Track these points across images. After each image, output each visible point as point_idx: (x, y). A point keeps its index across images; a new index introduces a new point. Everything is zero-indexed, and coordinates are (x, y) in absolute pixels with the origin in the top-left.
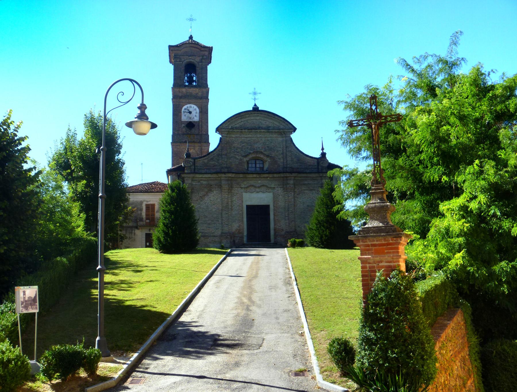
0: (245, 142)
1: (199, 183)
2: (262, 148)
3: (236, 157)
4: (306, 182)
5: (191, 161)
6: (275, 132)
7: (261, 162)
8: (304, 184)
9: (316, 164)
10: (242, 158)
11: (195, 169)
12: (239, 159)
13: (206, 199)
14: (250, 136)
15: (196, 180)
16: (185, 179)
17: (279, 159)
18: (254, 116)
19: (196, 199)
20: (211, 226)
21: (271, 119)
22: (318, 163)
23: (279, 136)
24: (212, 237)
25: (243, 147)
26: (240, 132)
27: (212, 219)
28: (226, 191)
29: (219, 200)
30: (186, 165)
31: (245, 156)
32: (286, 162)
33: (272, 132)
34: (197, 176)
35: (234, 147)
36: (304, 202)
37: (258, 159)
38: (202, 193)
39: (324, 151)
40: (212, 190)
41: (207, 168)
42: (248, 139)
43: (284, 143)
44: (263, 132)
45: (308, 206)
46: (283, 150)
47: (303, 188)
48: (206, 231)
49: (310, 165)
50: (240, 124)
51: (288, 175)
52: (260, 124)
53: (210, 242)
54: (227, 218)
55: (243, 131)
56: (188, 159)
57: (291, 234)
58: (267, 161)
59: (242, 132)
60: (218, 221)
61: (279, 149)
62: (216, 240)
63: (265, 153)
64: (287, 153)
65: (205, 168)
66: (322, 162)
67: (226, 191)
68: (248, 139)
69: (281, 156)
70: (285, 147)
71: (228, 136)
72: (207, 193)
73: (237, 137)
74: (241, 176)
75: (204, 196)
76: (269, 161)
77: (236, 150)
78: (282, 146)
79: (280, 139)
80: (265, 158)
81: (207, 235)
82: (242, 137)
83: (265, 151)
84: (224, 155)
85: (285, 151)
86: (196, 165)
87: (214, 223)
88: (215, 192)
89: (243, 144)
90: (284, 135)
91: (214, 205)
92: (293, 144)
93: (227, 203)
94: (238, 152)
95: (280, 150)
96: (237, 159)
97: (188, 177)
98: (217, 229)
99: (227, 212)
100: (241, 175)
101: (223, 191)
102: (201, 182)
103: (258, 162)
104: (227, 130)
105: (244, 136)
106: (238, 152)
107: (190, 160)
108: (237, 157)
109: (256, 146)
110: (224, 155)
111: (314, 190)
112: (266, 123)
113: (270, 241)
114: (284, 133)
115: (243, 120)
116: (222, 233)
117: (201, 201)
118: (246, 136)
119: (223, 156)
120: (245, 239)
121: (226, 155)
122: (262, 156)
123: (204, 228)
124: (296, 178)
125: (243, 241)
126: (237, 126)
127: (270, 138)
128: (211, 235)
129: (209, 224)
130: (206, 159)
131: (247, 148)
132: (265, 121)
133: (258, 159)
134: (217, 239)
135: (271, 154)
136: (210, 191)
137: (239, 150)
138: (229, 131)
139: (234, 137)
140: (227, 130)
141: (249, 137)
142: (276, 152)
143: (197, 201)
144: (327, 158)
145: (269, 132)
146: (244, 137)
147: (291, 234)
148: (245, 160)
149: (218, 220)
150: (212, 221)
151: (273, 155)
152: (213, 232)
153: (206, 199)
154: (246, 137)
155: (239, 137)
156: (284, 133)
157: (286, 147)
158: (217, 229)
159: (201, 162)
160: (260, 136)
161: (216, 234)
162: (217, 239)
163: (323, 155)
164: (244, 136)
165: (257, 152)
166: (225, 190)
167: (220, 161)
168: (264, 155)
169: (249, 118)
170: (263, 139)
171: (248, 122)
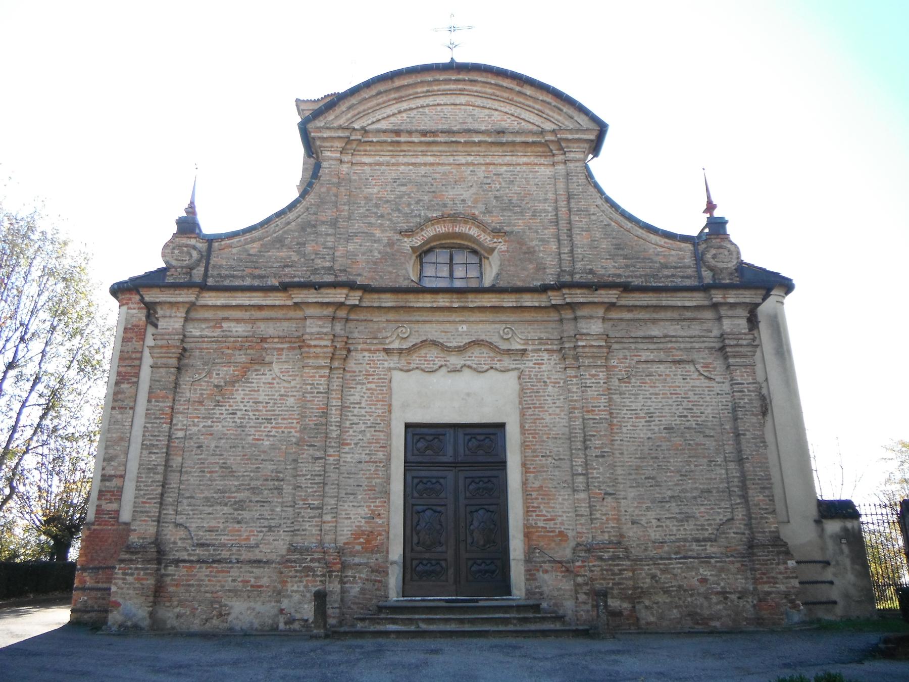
0: (410, 181)
1: (218, 332)
2: (476, 201)
3: (373, 235)
4: (655, 331)
5: (194, 248)
6: (526, 144)
7: (474, 259)
8: (650, 339)
9: (689, 260)
10: (398, 237)
11: (206, 275)
12: (385, 241)
13: (239, 398)
14: (431, 159)
15: (205, 320)
16: (160, 312)
17: (542, 240)
18: (445, 93)
19: (195, 397)
20: (246, 514)
21: (511, 102)
22: (699, 259)
23: (542, 160)
24: (247, 568)
25: (401, 197)
26: (393, 143)
27: (254, 484)
28: (322, 362)
29: (291, 401)
30: (174, 263)
31: (409, 233)
32: (572, 251)
33: (513, 143)
34: (211, 299)
35: (368, 199)
36: (650, 415)
37: (461, 247)
38: (223, 373)
39: (717, 213)
40: (267, 359)
41: (257, 272)
42: (423, 170)
43: (561, 185)
44: (480, 143)
45: (669, 429)
46: (556, 209)
47: (645, 355)
48: (224, 539)
49: (665, 266)
50: (392, 119)
51: (579, 296)
52: (470, 120)
53: (235, 592)
54: (318, 480)
55: (402, 139)
56: (184, 241)
57: (600, 558)
58: (492, 250)
59: (398, 143)
60: (280, 494)
61: (541, 206)
62: (265, 581)
63: (487, 219)
64: (575, 218)
65: (248, 271)
66: (713, 251)
67: (322, 362)
68: (423, 170)
69: (552, 230)
70: (563, 198)
71: (346, 158)
72: (245, 370)
73: (380, 164)
74: (388, 300)
75: (233, 383)
76: (504, 248)
77: (375, 210)
78: (551, 196)
79: (545, 172)
80: (486, 239)
81: (225, 554)
82: (398, 164)
83: (488, 211)
84: (323, 223)
85: (563, 211)
86: (214, 261)
87: (263, 503)
88: (276, 367)
89: (404, 189)
90: (560, 158)
91: (269, 420)
92: (596, 186)
93: (325, 414)
94: (382, 216)
95: (546, 211)
96: (378, 241)
97: (172, 304)
98: (270, 528)
99: (319, 454)
100: (388, 296)
101: (311, 362)
102: (225, 325)
103: (459, 258)
104: (340, 134)
105: (406, 160)
106: (382, 216)
107: (193, 242)
108: (378, 233)
109: (451, 193)
110: (323, 223)
111: (692, 362)
112: (490, 116)
113: (505, 588)
114: (561, 149)
115: (404, 105)
116: (293, 549)
117: (218, 404)
118: (413, 160)
119: (323, 229)
120: (394, 579)
121: (334, 223)
122: (474, 232)
123: (213, 523)
124: (614, 315)
125: (386, 586)
126: (383, 125)
127: (505, 168)
128: (246, 555)
129: (240, 505)
130: (253, 241)
131: (418, 202)
132: (487, 111)
133: (461, 247)
134: (266, 577)
135: (509, 224)
136: (259, 362)
137: (385, 209)
138: (348, 141)
139: (370, 164)
140: (340, 134)
141: (425, 164)
142: (528, 215)
143: (201, 403)
144: (733, 238)
145: (502, 144)
146: (409, 164)
147: (600, 558)
148: (408, 243)
149: (279, 489)
150: (254, 490)
151: (516, 229)
152: (252, 541)
153: (239, 398)
154: (414, 164)
155: (388, 164)
156: (561, 149)
157: (569, 197)
158: (270, 528)
159: (234, 251)
160: (470, 159)
161: (263, 552)
162: (266, 577)
163: (717, 227)
164: (406, 160)
165: (454, 218)
166: (317, 357)
167: (309, 248)
168: (481, 225)
169: (429, 101)
170: (481, 172)
171: (423, 114)
